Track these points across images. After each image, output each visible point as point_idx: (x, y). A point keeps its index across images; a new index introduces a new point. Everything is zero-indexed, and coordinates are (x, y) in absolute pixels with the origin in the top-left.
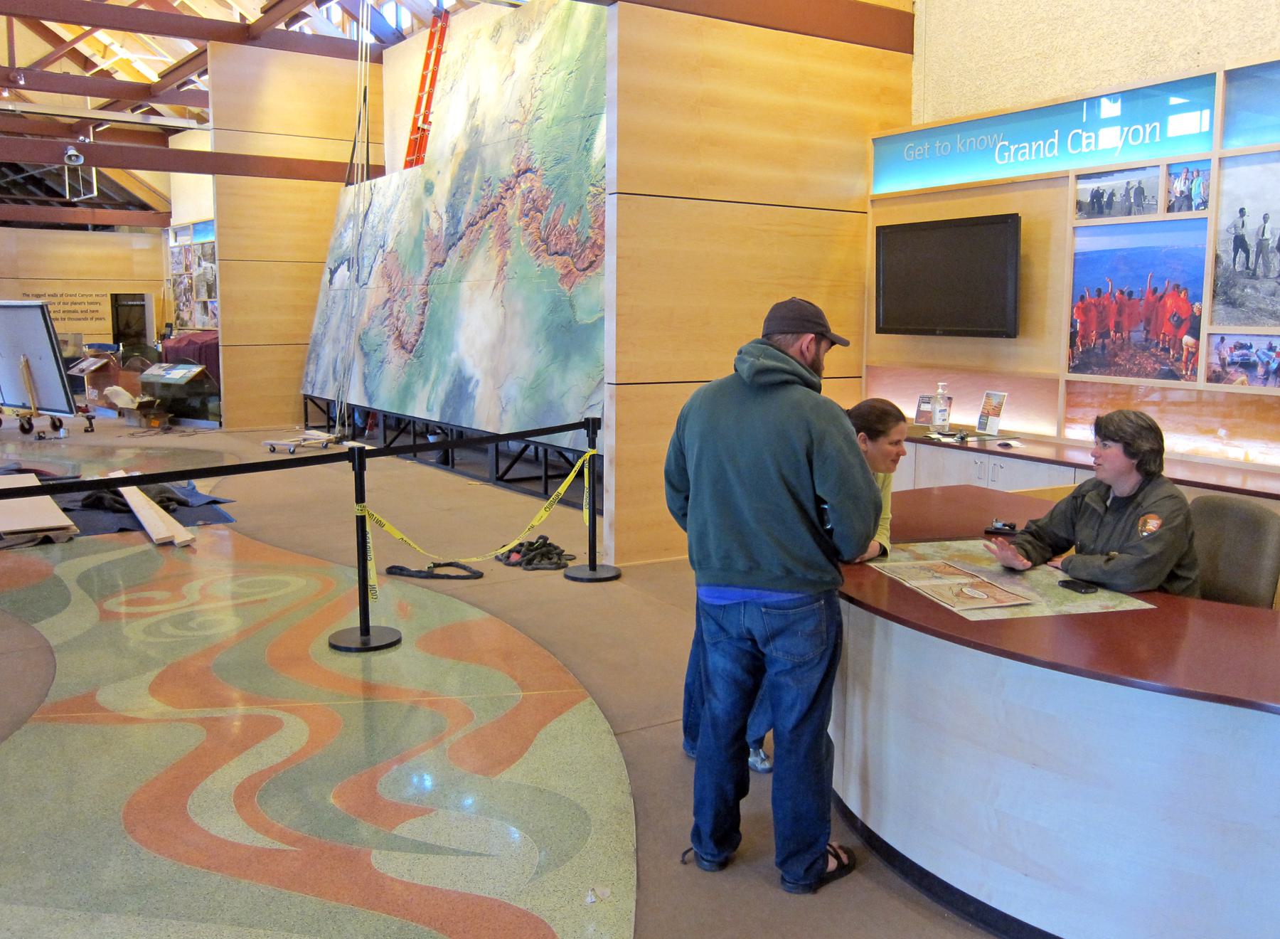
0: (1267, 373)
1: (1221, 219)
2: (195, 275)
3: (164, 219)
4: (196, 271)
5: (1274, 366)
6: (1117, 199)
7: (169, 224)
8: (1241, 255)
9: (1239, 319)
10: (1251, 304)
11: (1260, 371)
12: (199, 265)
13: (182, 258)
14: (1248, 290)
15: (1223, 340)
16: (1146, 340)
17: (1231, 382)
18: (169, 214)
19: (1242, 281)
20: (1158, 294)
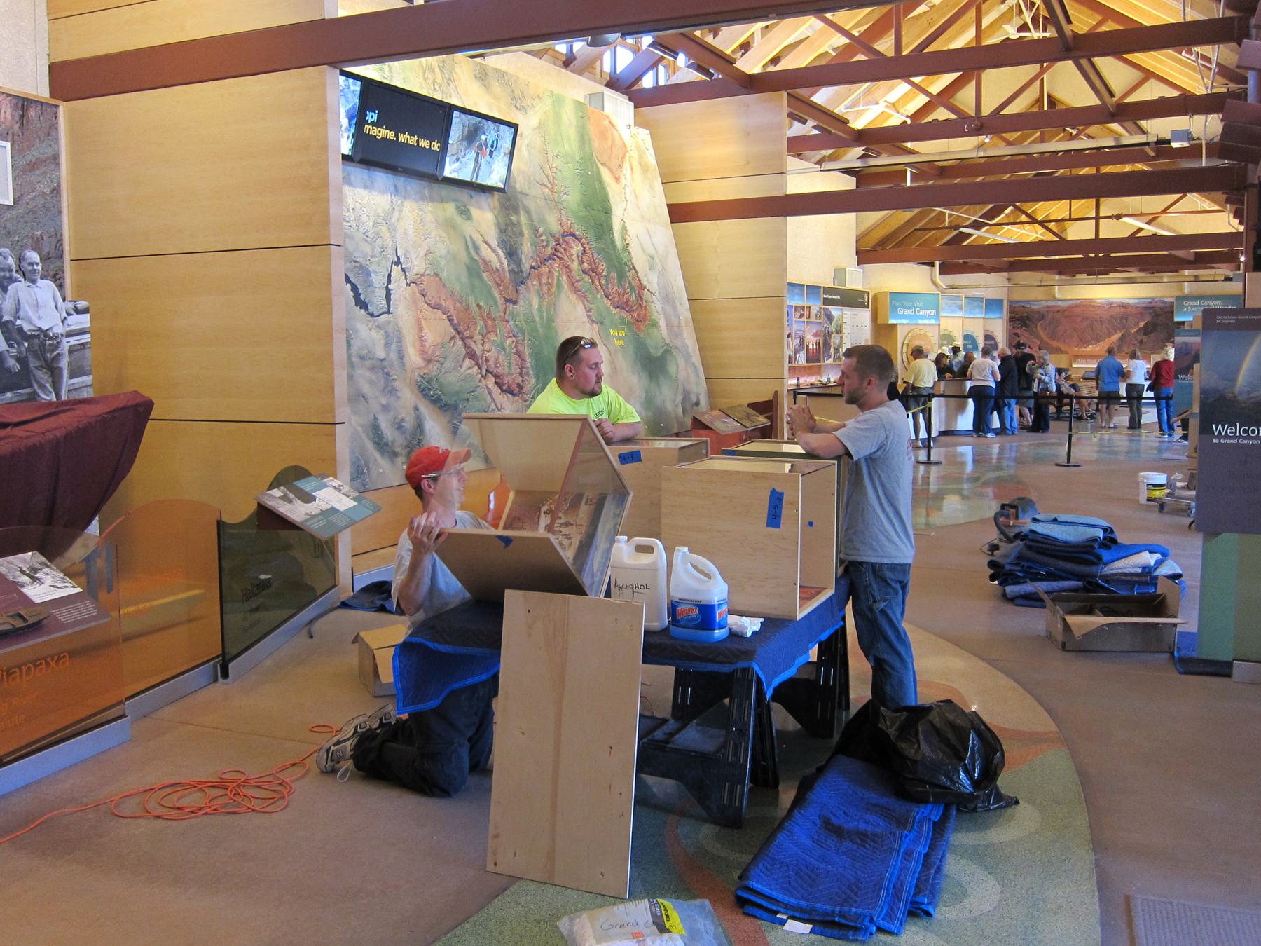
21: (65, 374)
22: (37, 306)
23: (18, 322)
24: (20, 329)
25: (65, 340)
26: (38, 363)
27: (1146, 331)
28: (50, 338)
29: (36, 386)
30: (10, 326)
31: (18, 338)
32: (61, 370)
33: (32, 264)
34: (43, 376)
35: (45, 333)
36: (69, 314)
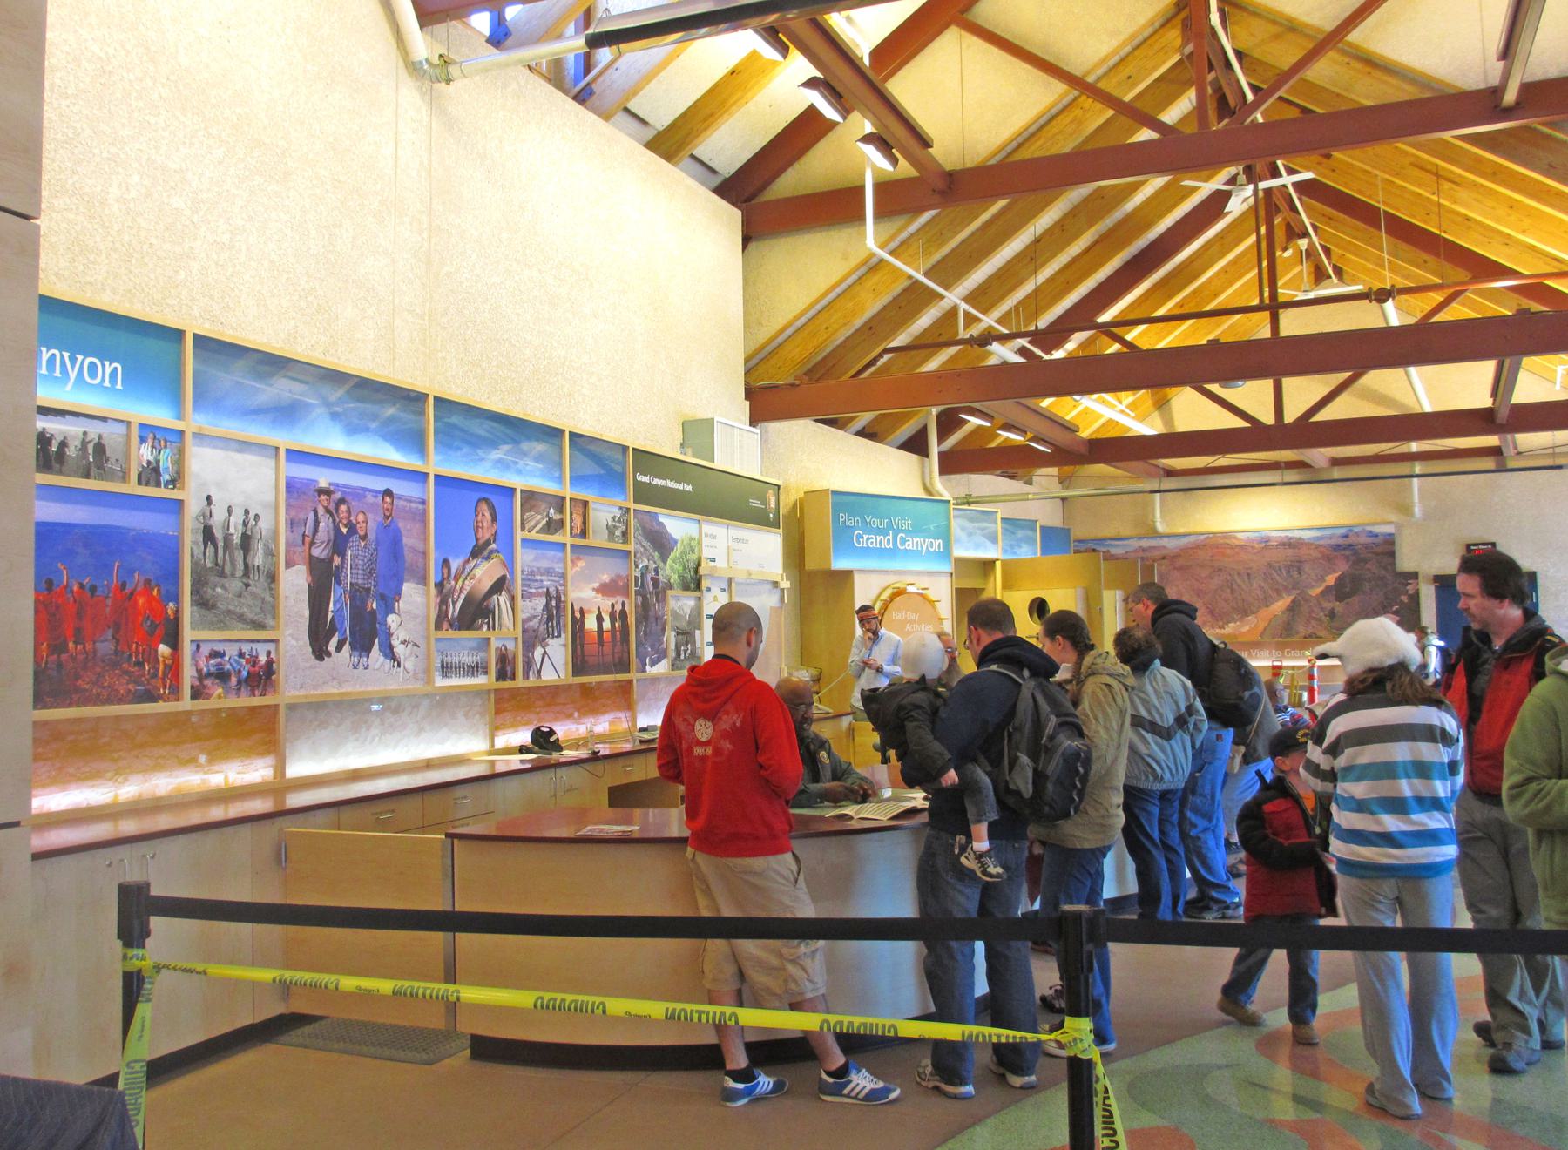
0: (239, 682)
1: (193, 507)
5: (245, 673)
6: (71, 451)
8: (210, 549)
9: (212, 623)
10: (221, 606)
11: (234, 680)
14: (219, 590)
15: (198, 647)
16: (116, 652)
17: (208, 696)
19: (213, 579)
20: (129, 588)
27: (1341, 591)
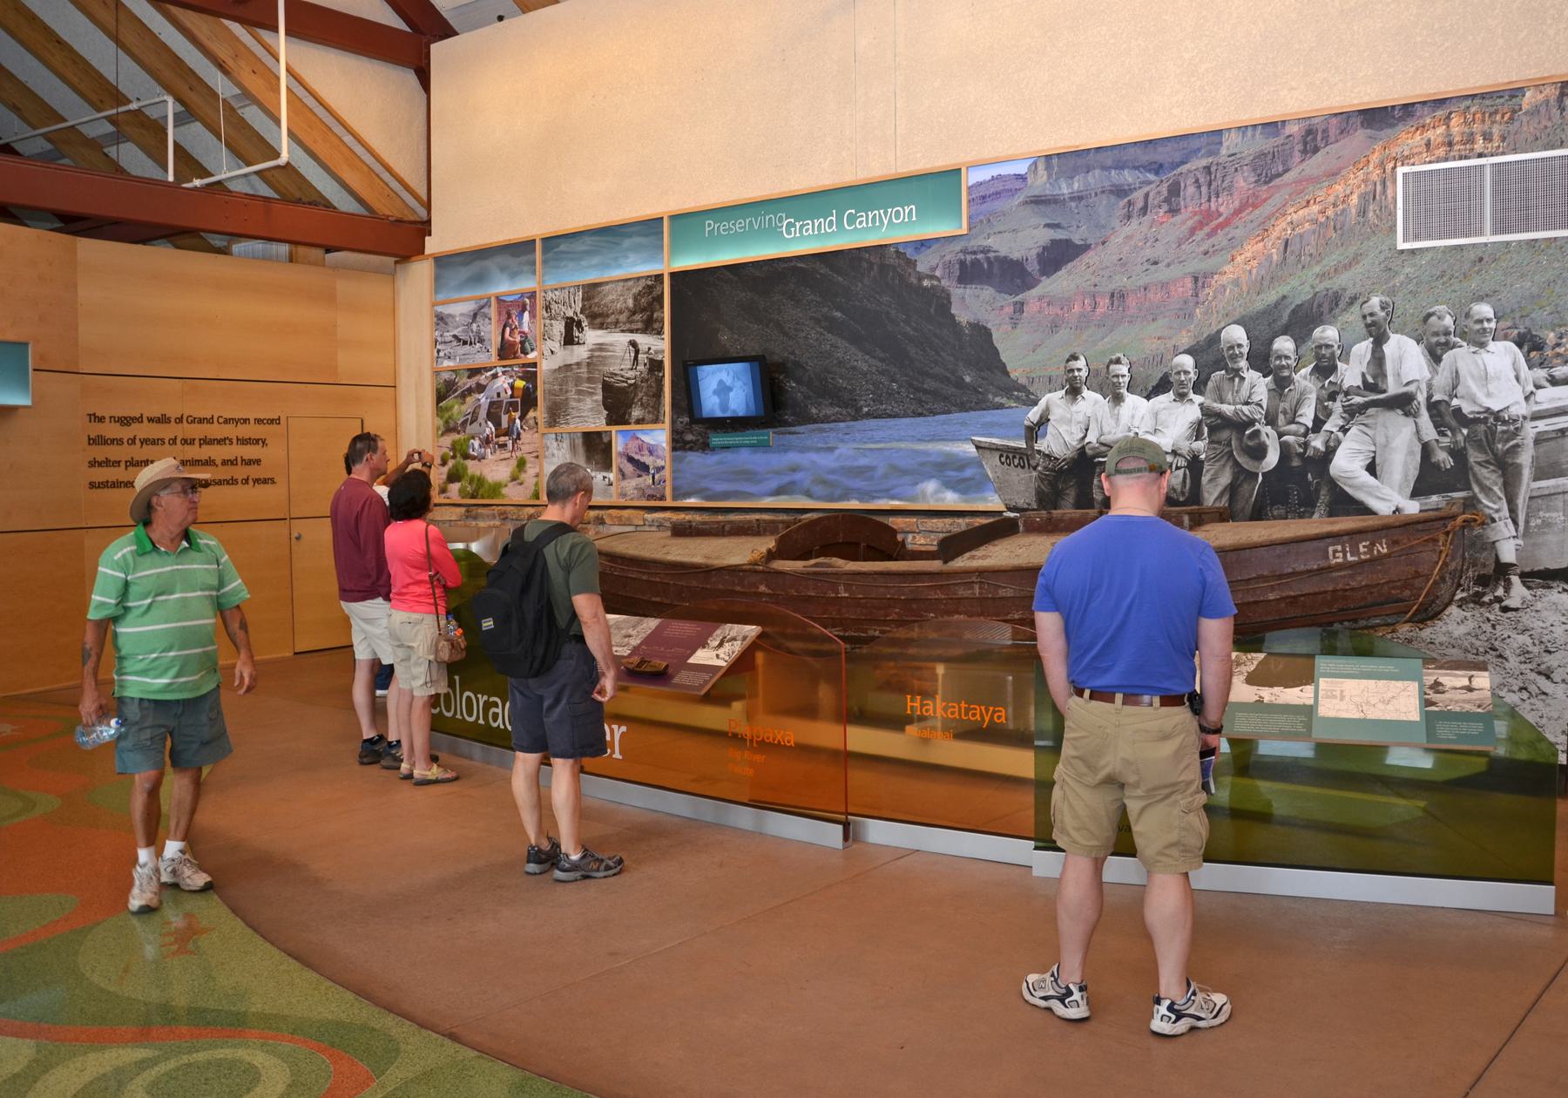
2: (546, 366)
3: (401, 236)
4: (549, 357)
7: (420, 250)
12: (569, 340)
13: (491, 331)
18: (425, 228)
21: (1526, 473)
22: (1485, 378)
23: (1455, 402)
24: (1458, 410)
25: (1529, 425)
26: (1481, 457)
28: (1505, 422)
29: (1476, 489)
30: (1442, 408)
31: (1454, 423)
32: (1518, 467)
33: (1481, 321)
34: (1490, 477)
35: (1497, 416)
36: (1538, 387)
